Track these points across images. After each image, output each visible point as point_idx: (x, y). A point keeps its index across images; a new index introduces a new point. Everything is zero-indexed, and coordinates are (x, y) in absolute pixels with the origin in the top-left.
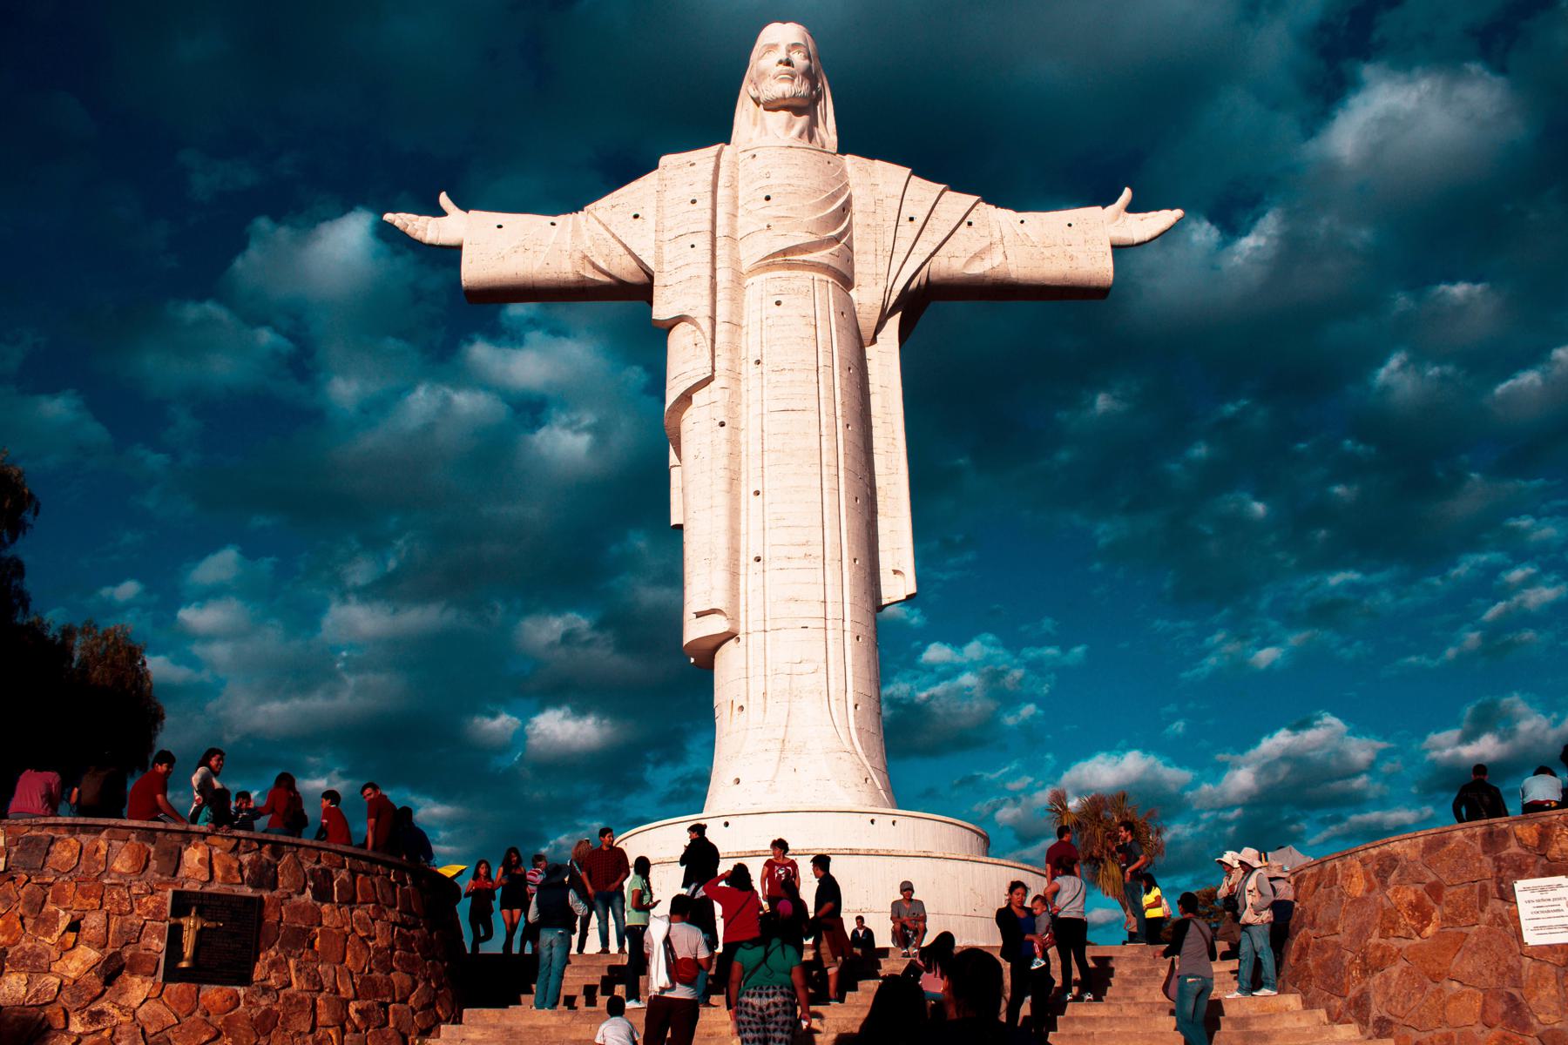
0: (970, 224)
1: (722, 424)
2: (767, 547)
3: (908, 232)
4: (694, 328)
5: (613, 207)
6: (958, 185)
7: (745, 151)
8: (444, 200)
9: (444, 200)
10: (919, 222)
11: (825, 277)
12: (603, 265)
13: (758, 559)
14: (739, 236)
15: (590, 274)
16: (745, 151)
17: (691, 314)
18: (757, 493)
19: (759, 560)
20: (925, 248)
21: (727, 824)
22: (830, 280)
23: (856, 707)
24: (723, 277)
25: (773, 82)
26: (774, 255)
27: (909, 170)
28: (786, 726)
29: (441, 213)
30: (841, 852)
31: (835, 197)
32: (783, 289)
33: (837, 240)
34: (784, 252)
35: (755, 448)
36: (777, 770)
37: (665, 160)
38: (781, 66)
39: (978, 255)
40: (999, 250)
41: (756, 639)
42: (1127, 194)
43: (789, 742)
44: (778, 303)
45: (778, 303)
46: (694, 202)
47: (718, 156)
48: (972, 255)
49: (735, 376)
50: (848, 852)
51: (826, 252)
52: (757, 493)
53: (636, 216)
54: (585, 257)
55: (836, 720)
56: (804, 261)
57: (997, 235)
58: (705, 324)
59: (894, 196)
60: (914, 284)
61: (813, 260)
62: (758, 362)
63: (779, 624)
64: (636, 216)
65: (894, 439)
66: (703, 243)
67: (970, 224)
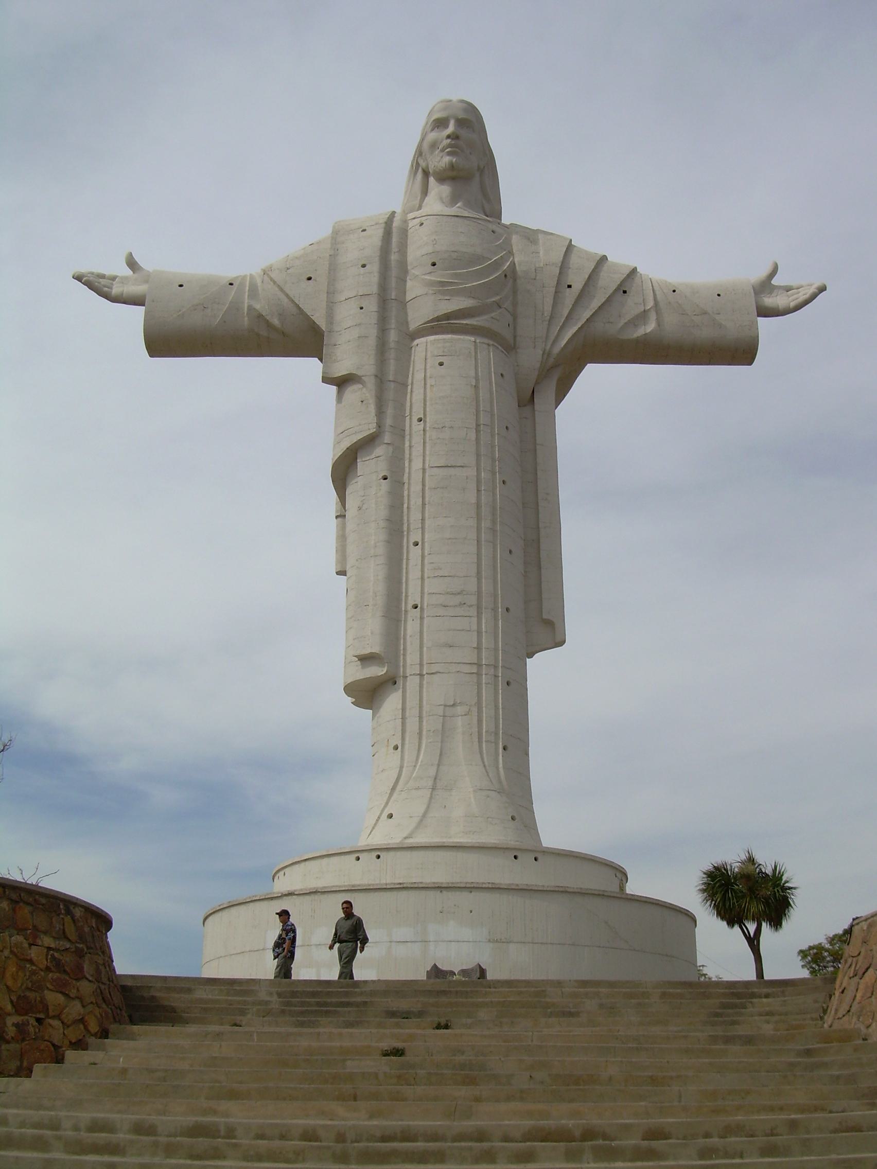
0: (625, 292)
1: (385, 479)
2: (426, 596)
4: (361, 386)
5: (288, 269)
7: (414, 218)
10: (578, 286)
11: (486, 341)
12: (276, 322)
13: (416, 607)
14: (408, 298)
16: (414, 218)
17: (359, 373)
18: (416, 544)
19: (416, 607)
21: (378, 857)
22: (491, 342)
23: (505, 748)
24: (393, 336)
25: (441, 154)
26: (438, 319)
28: (439, 765)
30: (484, 886)
31: (497, 264)
32: (445, 350)
33: (498, 305)
34: (448, 316)
35: (416, 502)
36: (428, 807)
38: (449, 141)
40: (653, 316)
41: (412, 683)
43: (440, 780)
44: (441, 364)
45: (441, 364)
46: (364, 266)
48: (626, 321)
49: (400, 432)
50: (490, 886)
51: (485, 317)
52: (416, 544)
53: (309, 279)
55: (485, 760)
56: (467, 324)
57: (650, 304)
58: (371, 382)
59: (553, 264)
61: (475, 323)
62: (420, 420)
63: (435, 668)
64: (309, 279)
65: (548, 494)
66: (372, 306)
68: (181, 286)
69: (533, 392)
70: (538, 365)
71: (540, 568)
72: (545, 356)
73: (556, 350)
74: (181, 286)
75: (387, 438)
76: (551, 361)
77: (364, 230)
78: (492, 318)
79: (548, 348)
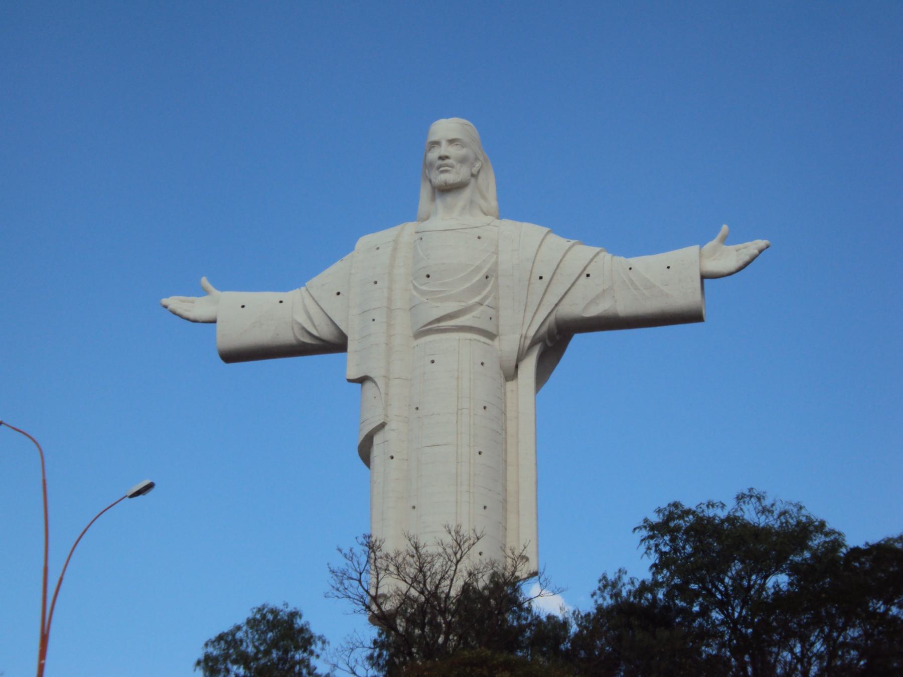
3: (540, 287)
6: (586, 241)
8: (204, 281)
9: (204, 281)
10: (547, 278)
15: (307, 340)
20: (551, 300)
27: (546, 230)
29: (204, 292)
31: (478, 269)
34: (439, 320)
37: (365, 242)
39: (595, 300)
42: (725, 228)
44: (433, 362)
47: (396, 241)
53: (338, 294)
54: (304, 329)
60: (544, 329)
64: (338, 294)
67: (588, 275)
68: (243, 307)
69: (517, 367)
70: (517, 348)
71: (518, 512)
72: (523, 340)
73: (532, 333)
74: (243, 307)
75: (392, 425)
76: (528, 342)
77: (378, 248)
78: (474, 317)
79: (524, 332)
